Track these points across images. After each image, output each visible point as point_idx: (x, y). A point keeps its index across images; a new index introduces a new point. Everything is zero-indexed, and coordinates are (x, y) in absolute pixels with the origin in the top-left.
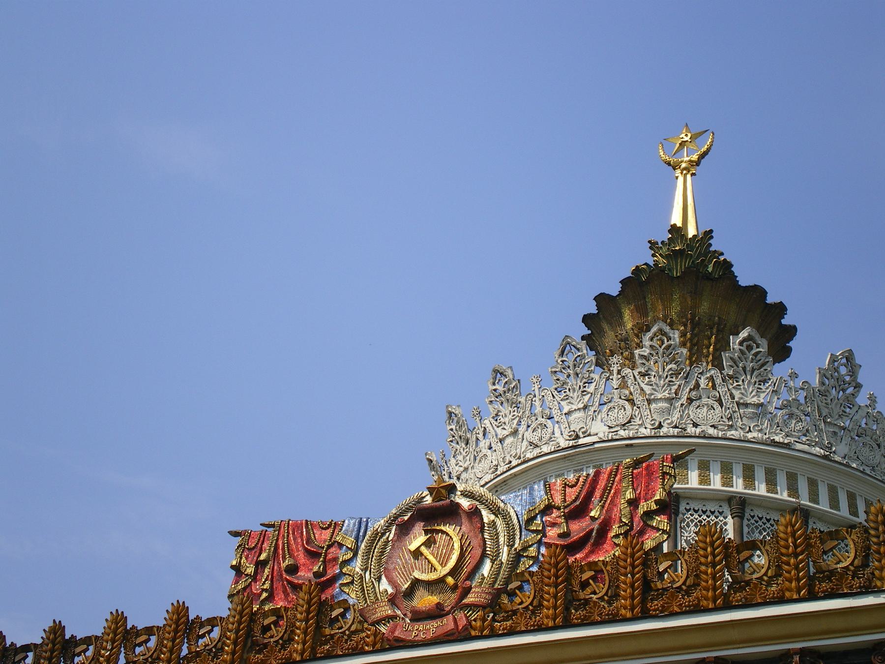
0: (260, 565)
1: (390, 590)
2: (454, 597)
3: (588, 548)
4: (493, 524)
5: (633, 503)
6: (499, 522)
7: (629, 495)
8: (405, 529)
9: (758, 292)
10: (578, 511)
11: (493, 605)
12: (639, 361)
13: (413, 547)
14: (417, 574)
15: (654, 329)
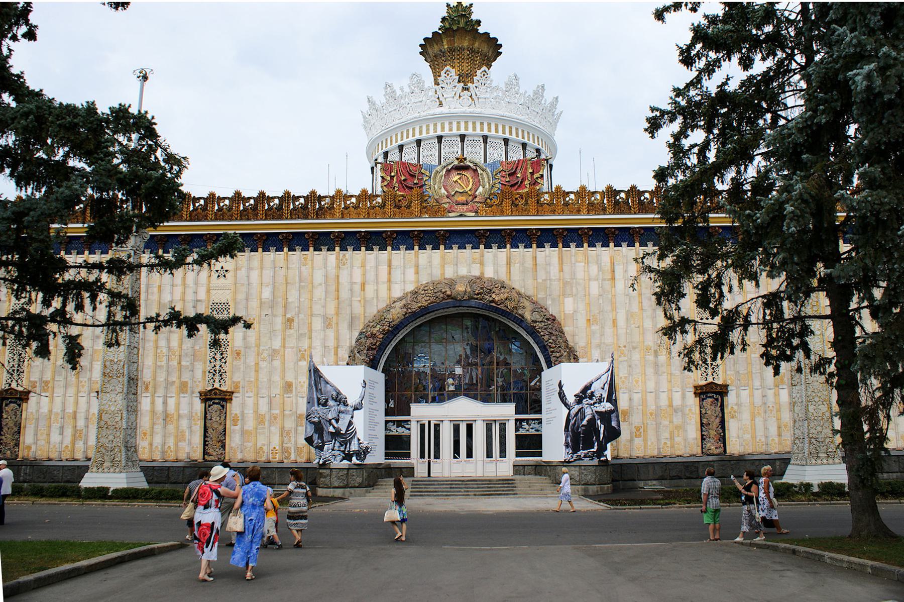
0: (392, 177)
1: (446, 193)
2: (471, 198)
3: (517, 186)
4: (481, 174)
5: (532, 174)
6: (484, 174)
7: (531, 171)
8: (448, 171)
9: (496, 40)
10: (511, 175)
11: (485, 202)
12: (475, 81)
13: (455, 179)
14: (457, 189)
15: (482, 69)
